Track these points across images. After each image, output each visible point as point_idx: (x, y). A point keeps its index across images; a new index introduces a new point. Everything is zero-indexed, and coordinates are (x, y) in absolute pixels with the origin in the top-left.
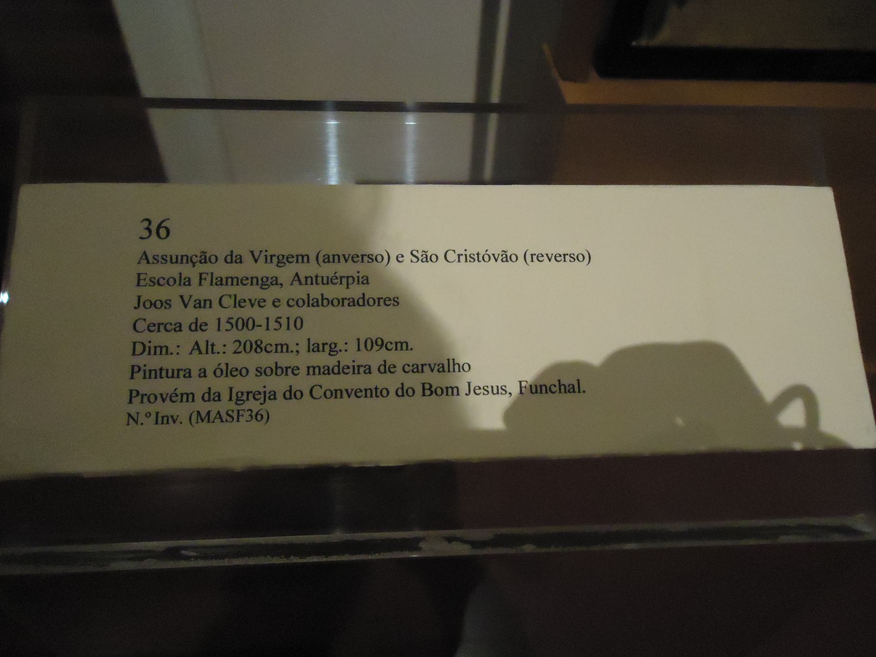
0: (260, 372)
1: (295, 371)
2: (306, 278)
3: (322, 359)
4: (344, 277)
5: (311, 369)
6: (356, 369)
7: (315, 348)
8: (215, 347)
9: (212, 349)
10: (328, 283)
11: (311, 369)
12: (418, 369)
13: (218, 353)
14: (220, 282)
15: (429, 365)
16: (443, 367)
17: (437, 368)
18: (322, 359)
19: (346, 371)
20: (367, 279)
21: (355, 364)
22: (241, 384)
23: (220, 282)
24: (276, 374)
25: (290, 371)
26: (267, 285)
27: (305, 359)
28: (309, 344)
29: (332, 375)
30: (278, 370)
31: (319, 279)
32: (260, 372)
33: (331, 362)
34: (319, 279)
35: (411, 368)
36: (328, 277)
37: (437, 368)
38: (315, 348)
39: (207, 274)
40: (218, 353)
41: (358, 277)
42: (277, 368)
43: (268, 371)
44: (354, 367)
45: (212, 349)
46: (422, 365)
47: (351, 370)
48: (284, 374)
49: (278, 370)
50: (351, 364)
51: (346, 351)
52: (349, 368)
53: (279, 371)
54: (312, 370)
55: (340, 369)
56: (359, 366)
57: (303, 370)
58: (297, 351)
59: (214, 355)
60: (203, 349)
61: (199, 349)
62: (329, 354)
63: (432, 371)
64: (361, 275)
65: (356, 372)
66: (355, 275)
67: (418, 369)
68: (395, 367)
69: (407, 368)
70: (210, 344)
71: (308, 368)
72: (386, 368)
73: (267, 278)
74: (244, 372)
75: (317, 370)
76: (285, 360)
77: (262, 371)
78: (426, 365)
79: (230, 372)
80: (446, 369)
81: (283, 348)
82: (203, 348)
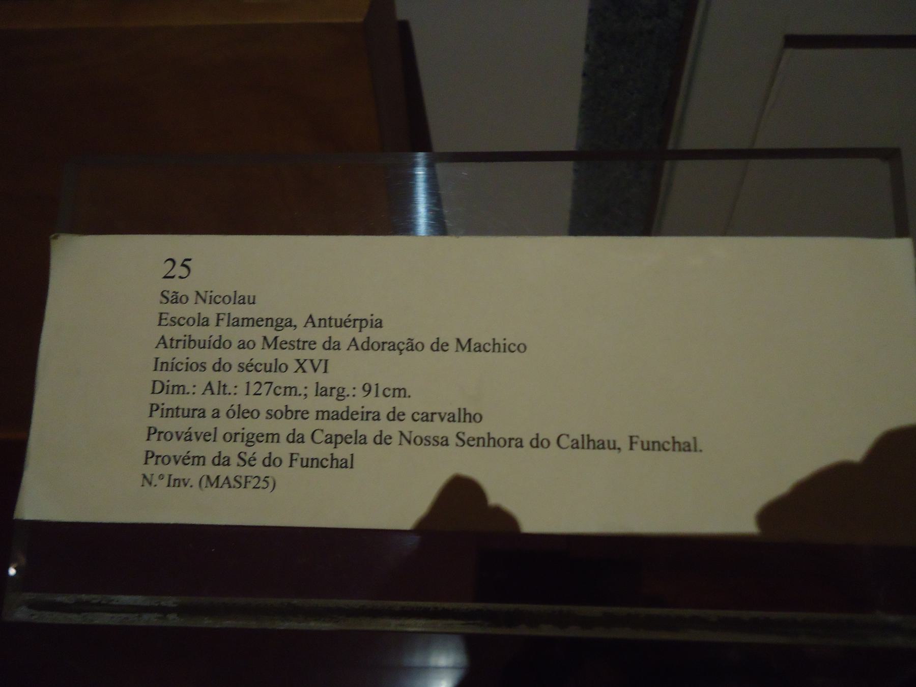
0: (271, 415)
1: (304, 414)
2: (320, 320)
3: (330, 404)
4: (357, 320)
5: (320, 414)
6: (366, 415)
7: (323, 392)
8: (226, 388)
9: (224, 389)
10: (341, 326)
11: (320, 414)
12: (427, 418)
13: (230, 394)
14: (237, 323)
15: (440, 414)
16: (454, 416)
17: (447, 417)
18: (330, 404)
19: (355, 417)
20: (381, 322)
21: (365, 410)
22: (252, 426)
23: (237, 323)
24: (286, 417)
25: (299, 414)
26: (281, 326)
27: (314, 404)
28: (317, 387)
29: (340, 420)
30: (287, 413)
31: (333, 322)
32: (271, 415)
33: (341, 407)
34: (333, 322)
35: (420, 416)
36: (341, 319)
37: (447, 417)
38: (323, 392)
39: (224, 314)
40: (230, 394)
41: (372, 320)
42: (287, 411)
43: (279, 414)
44: (363, 412)
45: (224, 389)
46: (432, 414)
47: (360, 415)
48: (294, 417)
49: (287, 413)
50: (360, 410)
51: (354, 396)
52: (357, 414)
53: (289, 414)
54: (322, 414)
55: (350, 415)
56: (368, 413)
57: (313, 415)
58: (305, 395)
59: (226, 395)
60: (216, 390)
61: (211, 389)
62: (337, 399)
63: (442, 419)
64: (374, 318)
65: (365, 418)
66: (369, 318)
67: (428, 417)
68: (404, 414)
69: (416, 417)
70: (222, 384)
71: (318, 412)
72: (396, 416)
73: (282, 319)
74: (255, 414)
75: (326, 414)
76: (295, 403)
77: (273, 413)
78: (435, 413)
79: (242, 413)
80: (457, 418)
81: (290, 390)
82: (215, 388)
